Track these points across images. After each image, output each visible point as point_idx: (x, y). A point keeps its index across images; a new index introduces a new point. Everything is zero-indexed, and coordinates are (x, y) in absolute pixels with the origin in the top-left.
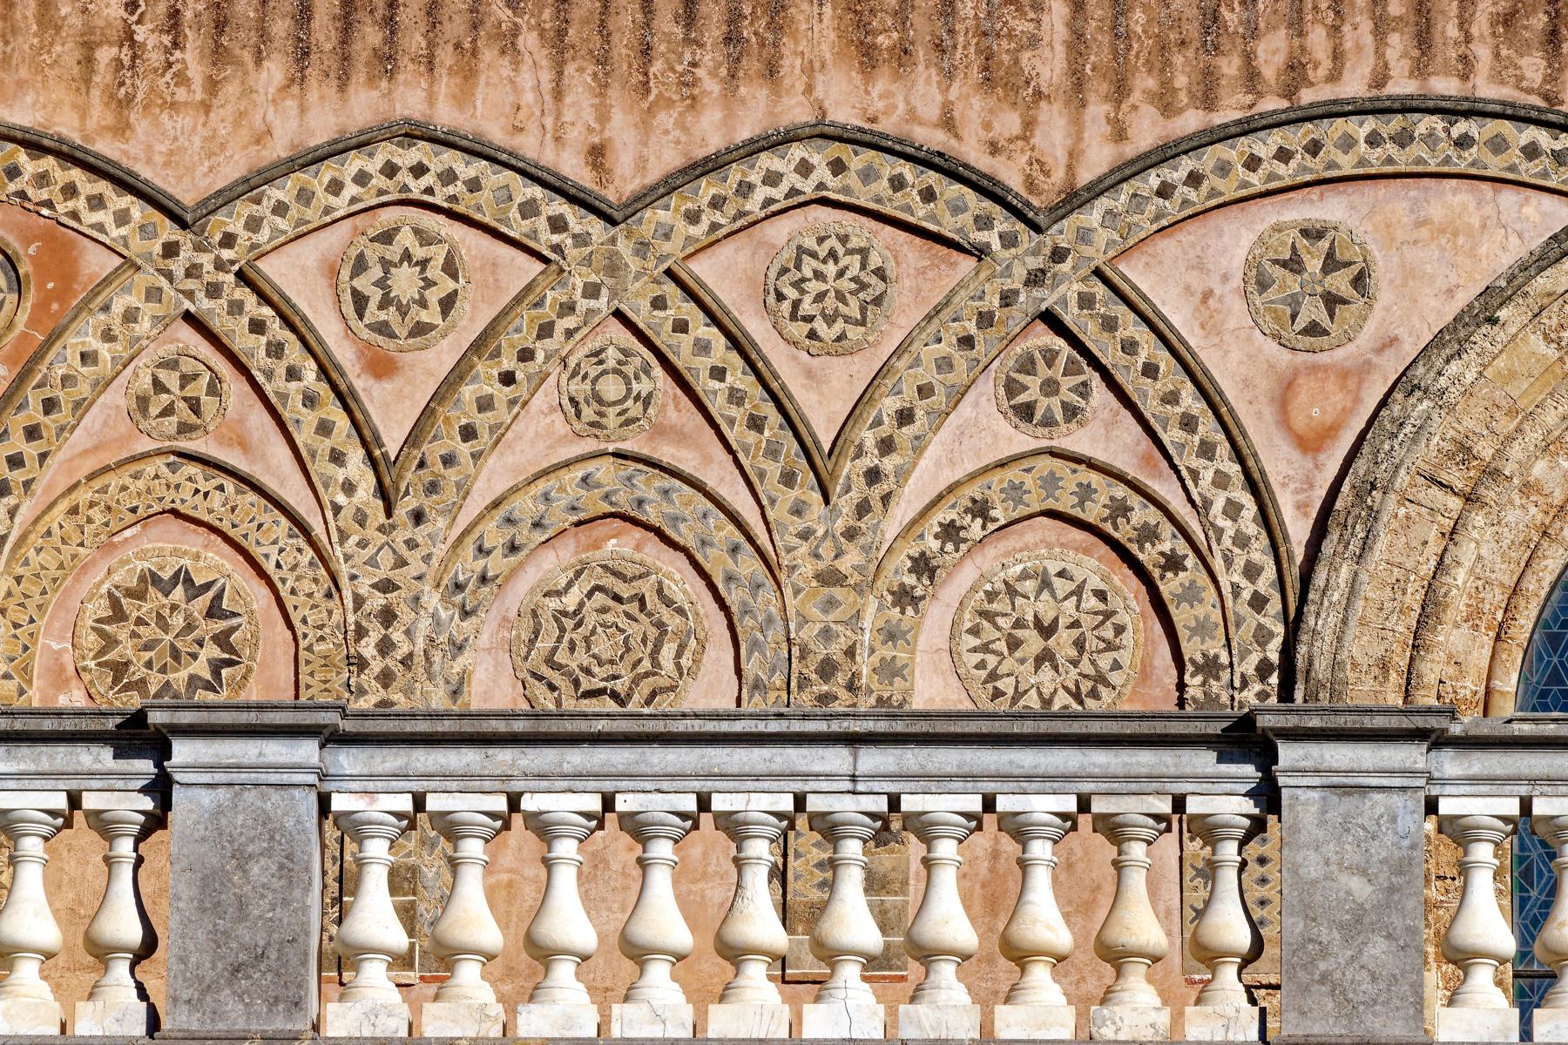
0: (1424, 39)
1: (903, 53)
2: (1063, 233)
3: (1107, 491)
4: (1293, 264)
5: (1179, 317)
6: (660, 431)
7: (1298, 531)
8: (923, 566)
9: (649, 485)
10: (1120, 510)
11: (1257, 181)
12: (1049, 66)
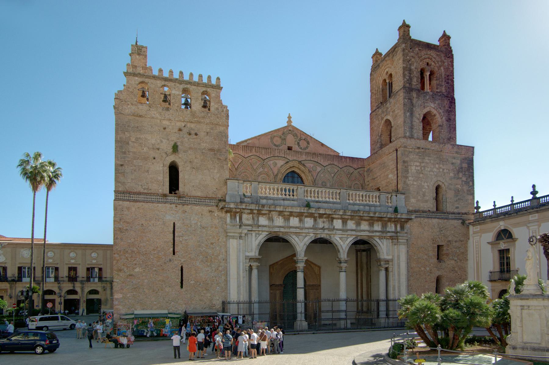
1: (257, 152)
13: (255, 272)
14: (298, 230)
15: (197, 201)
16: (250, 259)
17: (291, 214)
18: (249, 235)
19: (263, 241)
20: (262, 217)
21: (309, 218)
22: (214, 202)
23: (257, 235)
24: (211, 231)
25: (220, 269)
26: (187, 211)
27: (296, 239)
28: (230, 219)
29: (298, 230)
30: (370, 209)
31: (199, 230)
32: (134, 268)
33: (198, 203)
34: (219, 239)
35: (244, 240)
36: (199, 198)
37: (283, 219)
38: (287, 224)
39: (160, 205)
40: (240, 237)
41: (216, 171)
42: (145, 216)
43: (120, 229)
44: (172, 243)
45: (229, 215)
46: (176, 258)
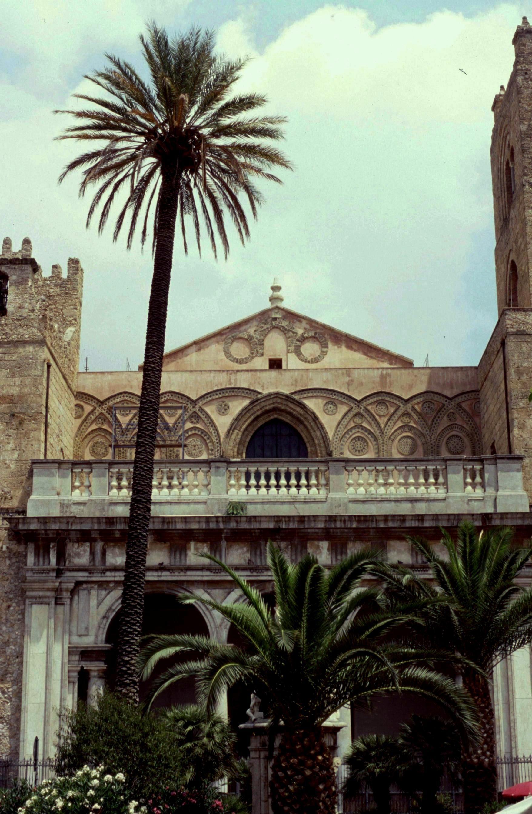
7: (222, 435)
11: (217, 397)
14: (208, 573)
18: (83, 594)
30: (413, 507)
34: (9, 607)
35: (67, 607)
40: (58, 601)
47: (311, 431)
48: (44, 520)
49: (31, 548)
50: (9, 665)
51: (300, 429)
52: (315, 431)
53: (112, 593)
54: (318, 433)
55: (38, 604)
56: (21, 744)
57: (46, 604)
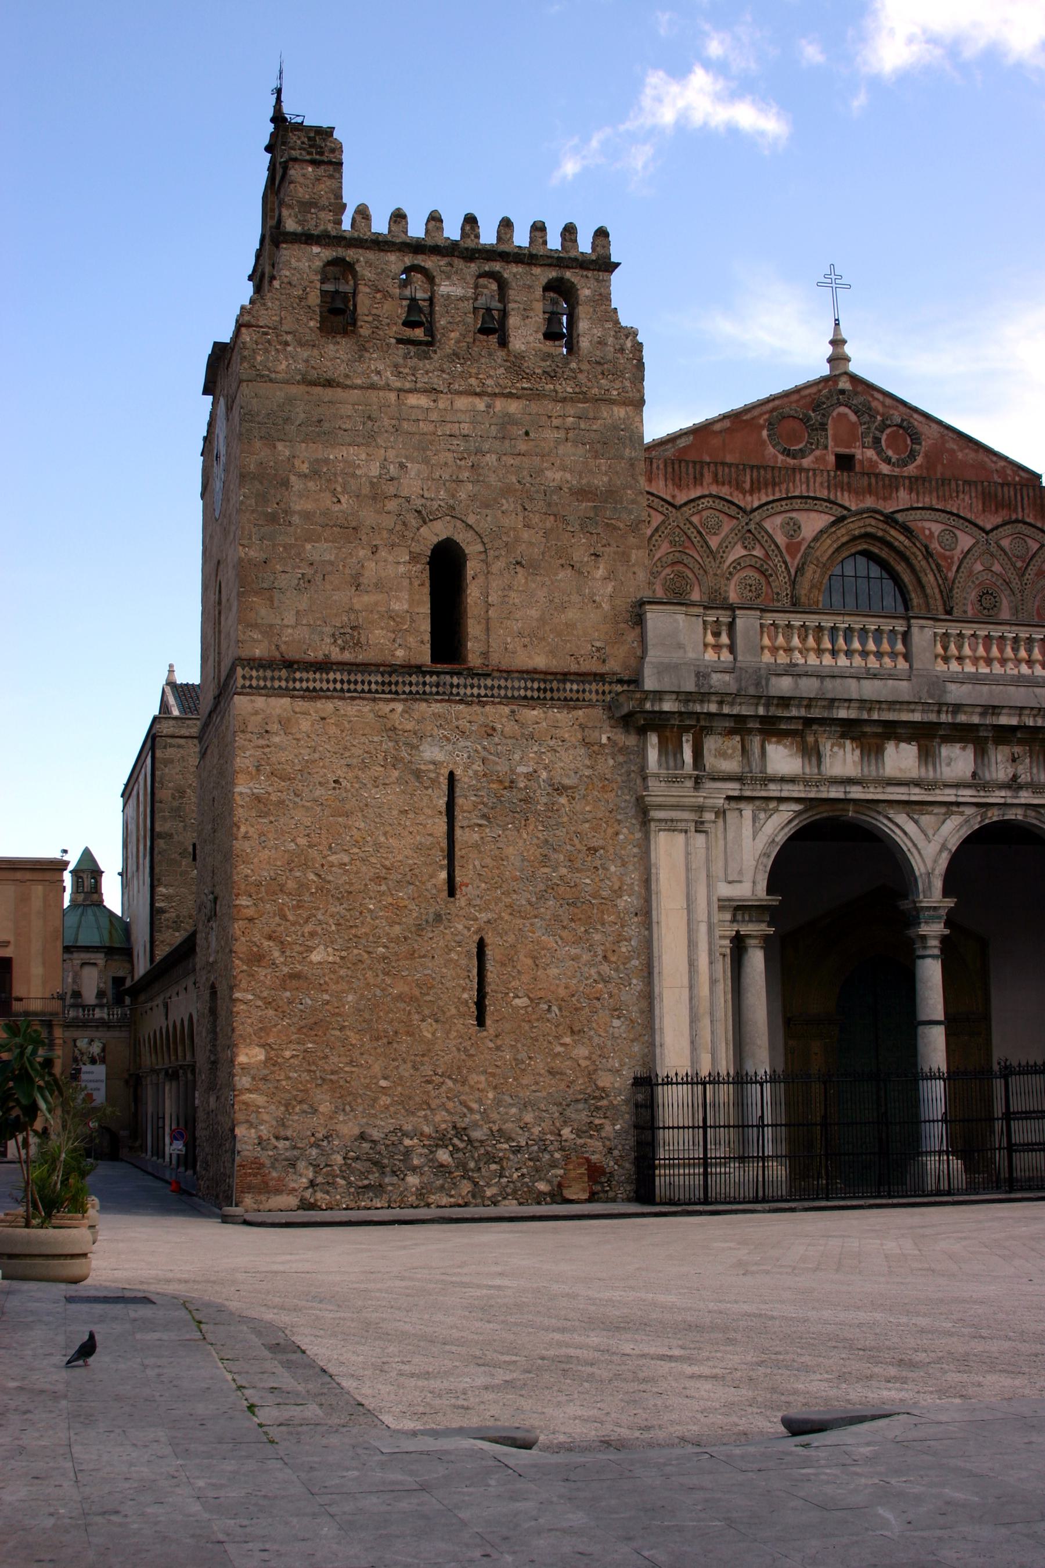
0: (808, 486)
2: (752, 516)
3: (760, 562)
4: (788, 524)
5: (770, 531)
6: (686, 548)
7: (793, 571)
8: (730, 573)
9: (685, 557)
10: (762, 565)
11: (782, 509)
12: (747, 486)
13: (756, 960)
14: (917, 790)
15: (532, 689)
16: (737, 908)
17: (893, 731)
19: (781, 838)
20: (778, 742)
21: (958, 745)
22: (597, 692)
23: (762, 815)
24: (588, 804)
25: (624, 950)
26: (499, 726)
27: (910, 827)
28: (660, 755)
29: (916, 794)
31: (544, 800)
32: (310, 949)
33: (536, 694)
34: (617, 834)
36: (542, 676)
37: (858, 752)
38: (873, 768)
39: (399, 707)
40: (700, 827)
41: (600, 573)
42: (345, 748)
43: (258, 799)
44: (442, 850)
45: (653, 739)
46: (461, 908)
47: (921, 575)
48: (687, 697)
49: (653, 739)
50: (622, 926)
51: (900, 568)
52: (926, 575)
53: (775, 817)
54: (931, 577)
55: (669, 830)
56: (658, 1051)
57: (681, 831)
